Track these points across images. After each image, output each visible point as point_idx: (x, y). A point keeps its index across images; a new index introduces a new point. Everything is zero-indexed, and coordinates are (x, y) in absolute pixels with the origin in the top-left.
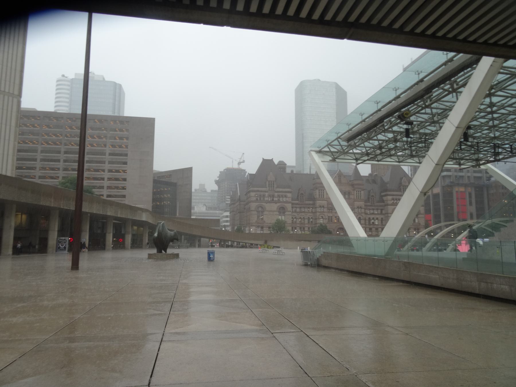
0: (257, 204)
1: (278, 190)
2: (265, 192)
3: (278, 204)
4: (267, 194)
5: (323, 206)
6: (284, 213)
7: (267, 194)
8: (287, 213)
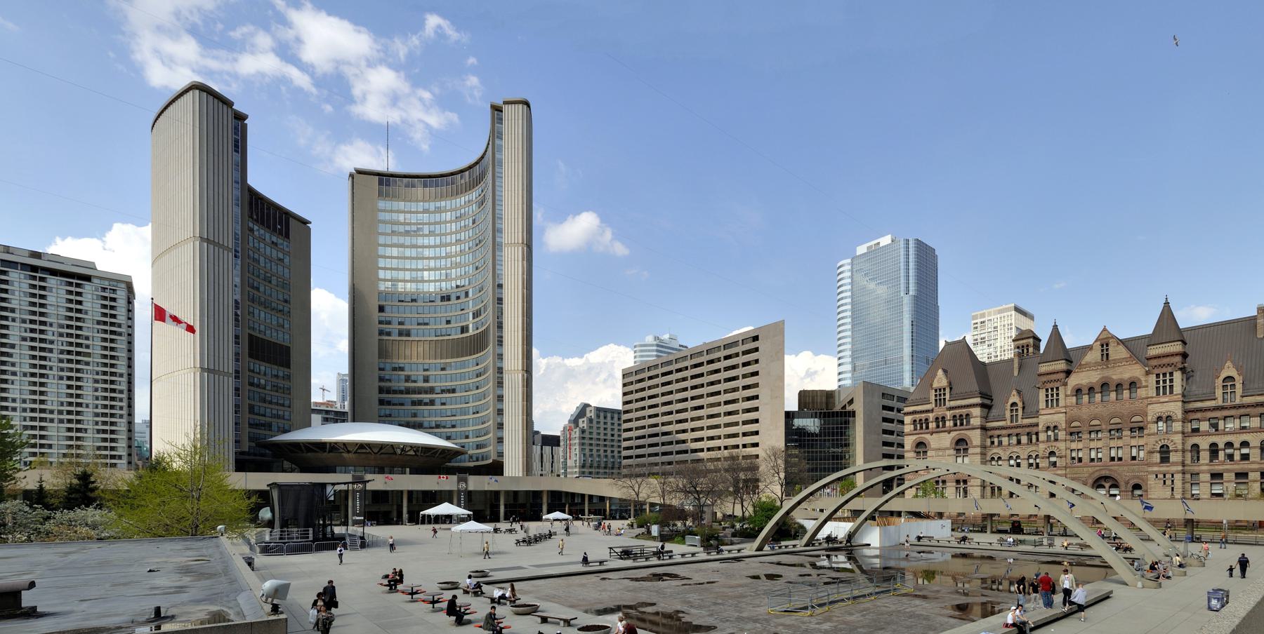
0: (914, 437)
1: (953, 404)
2: (927, 411)
3: (953, 434)
4: (931, 416)
5: (1055, 427)
6: (966, 450)
7: (931, 416)
8: (970, 451)
